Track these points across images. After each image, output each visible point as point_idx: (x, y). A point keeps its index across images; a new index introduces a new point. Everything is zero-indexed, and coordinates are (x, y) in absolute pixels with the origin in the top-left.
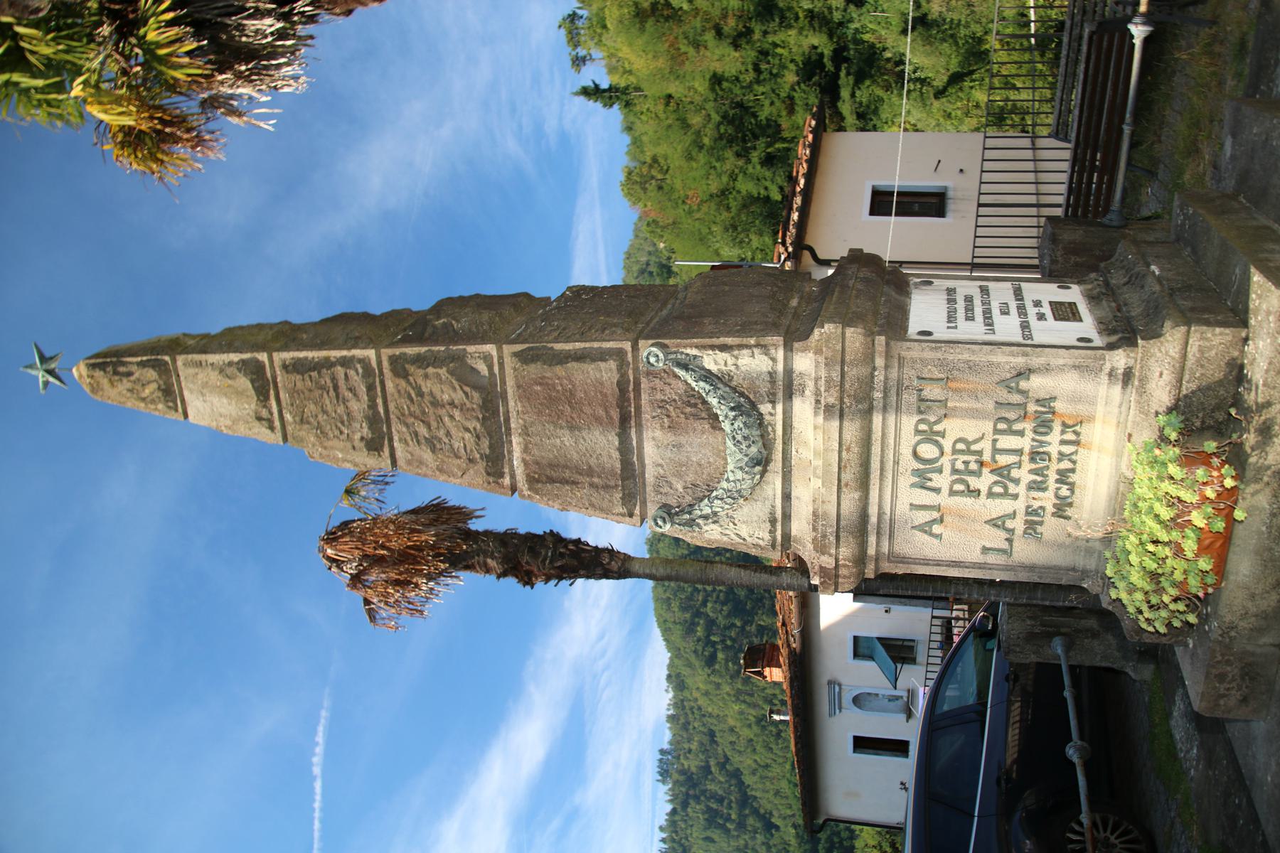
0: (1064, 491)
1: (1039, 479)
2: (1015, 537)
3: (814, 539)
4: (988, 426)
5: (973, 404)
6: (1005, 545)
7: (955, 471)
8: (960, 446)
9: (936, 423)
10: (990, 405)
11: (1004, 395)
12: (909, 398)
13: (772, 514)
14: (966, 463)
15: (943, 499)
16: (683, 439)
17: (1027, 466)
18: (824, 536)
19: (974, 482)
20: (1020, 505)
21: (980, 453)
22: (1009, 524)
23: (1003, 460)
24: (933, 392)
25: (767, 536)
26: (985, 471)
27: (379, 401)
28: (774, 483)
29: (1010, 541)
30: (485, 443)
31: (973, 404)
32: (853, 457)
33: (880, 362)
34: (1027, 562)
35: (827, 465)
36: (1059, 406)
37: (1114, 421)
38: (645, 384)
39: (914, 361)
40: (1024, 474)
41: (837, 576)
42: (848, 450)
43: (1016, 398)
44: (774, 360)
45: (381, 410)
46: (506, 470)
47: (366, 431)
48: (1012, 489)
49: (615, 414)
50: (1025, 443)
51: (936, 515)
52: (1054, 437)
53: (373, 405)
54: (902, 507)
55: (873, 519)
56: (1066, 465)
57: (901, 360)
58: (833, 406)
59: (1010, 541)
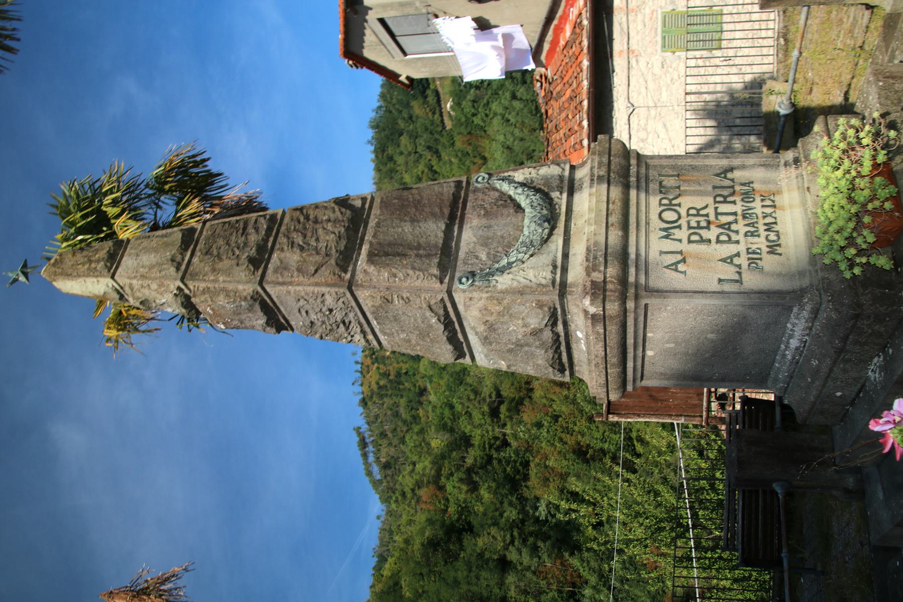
0: (772, 237)
1: (752, 229)
2: (742, 271)
4: (710, 200)
5: (698, 188)
6: (737, 277)
7: (690, 228)
8: (693, 212)
10: (710, 188)
11: (717, 181)
12: (653, 186)
14: (698, 222)
15: (684, 246)
16: (493, 222)
17: (741, 222)
18: (595, 258)
19: (705, 234)
20: (742, 248)
21: (707, 215)
22: (736, 261)
23: (724, 219)
24: (670, 182)
26: (712, 227)
27: (271, 239)
28: (558, 241)
29: (739, 273)
30: (343, 243)
31: (698, 188)
34: (755, 288)
36: (756, 186)
37: (796, 187)
38: (471, 197)
39: (655, 166)
41: (605, 290)
42: (613, 203)
45: (270, 244)
46: (350, 269)
47: (253, 252)
48: (734, 237)
49: (447, 211)
50: (738, 208)
51: (679, 257)
53: (265, 241)
54: (653, 254)
55: (633, 256)
56: (769, 220)
58: (603, 176)
59: (739, 273)
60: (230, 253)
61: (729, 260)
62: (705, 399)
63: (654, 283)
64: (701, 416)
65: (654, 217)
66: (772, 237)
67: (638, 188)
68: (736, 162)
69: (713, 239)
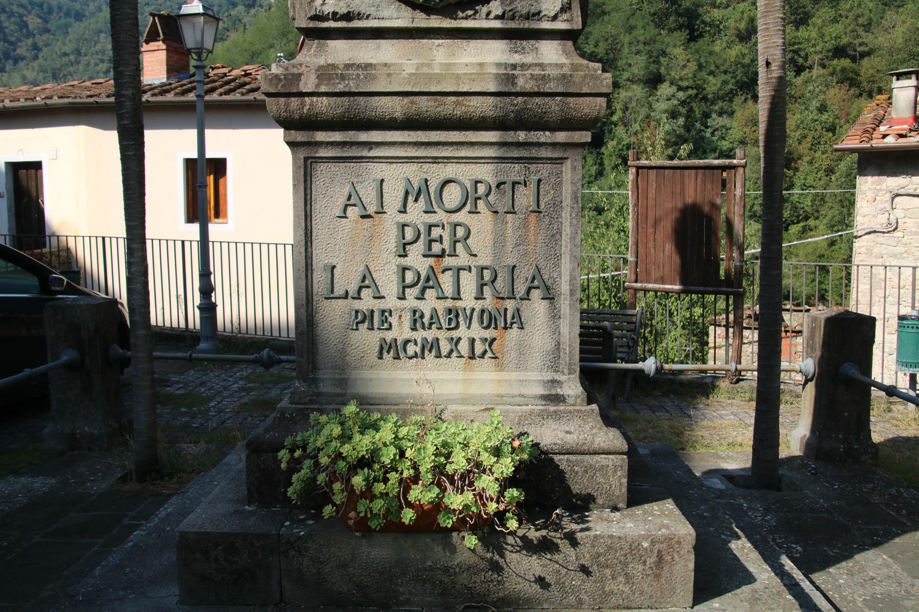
0: (411, 349)
1: (426, 320)
2: (350, 300)
3: (334, 66)
4: (485, 259)
6: (339, 291)
7: (430, 227)
8: (460, 232)
9: (489, 205)
10: (511, 262)
12: (515, 172)
13: (359, 16)
14: (441, 240)
15: (392, 217)
17: (441, 306)
18: (343, 78)
20: (391, 302)
21: (454, 254)
22: (365, 293)
23: (447, 281)
24: (525, 198)
25: (328, 9)
26: (431, 261)
29: (346, 296)
32: (449, 108)
33: (561, 137)
34: (318, 317)
35: (438, 78)
36: (514, 332)
37: (503, 392)
39: (559, 174)
40: (427, 306)
42: (458, 103)
43: (521, 289)
44: (555, 18)
48: (411, 293)
50: (468, 301)
52: (477, 331)
54: (379, 170)
55: (363, 137)
56: (445, 347)
57: (560, 160)
58: (514, 84)
59: (346, 296)
61: (367, 280)
63: (323, 172)
64: (636, 281)
65: (450, 170)
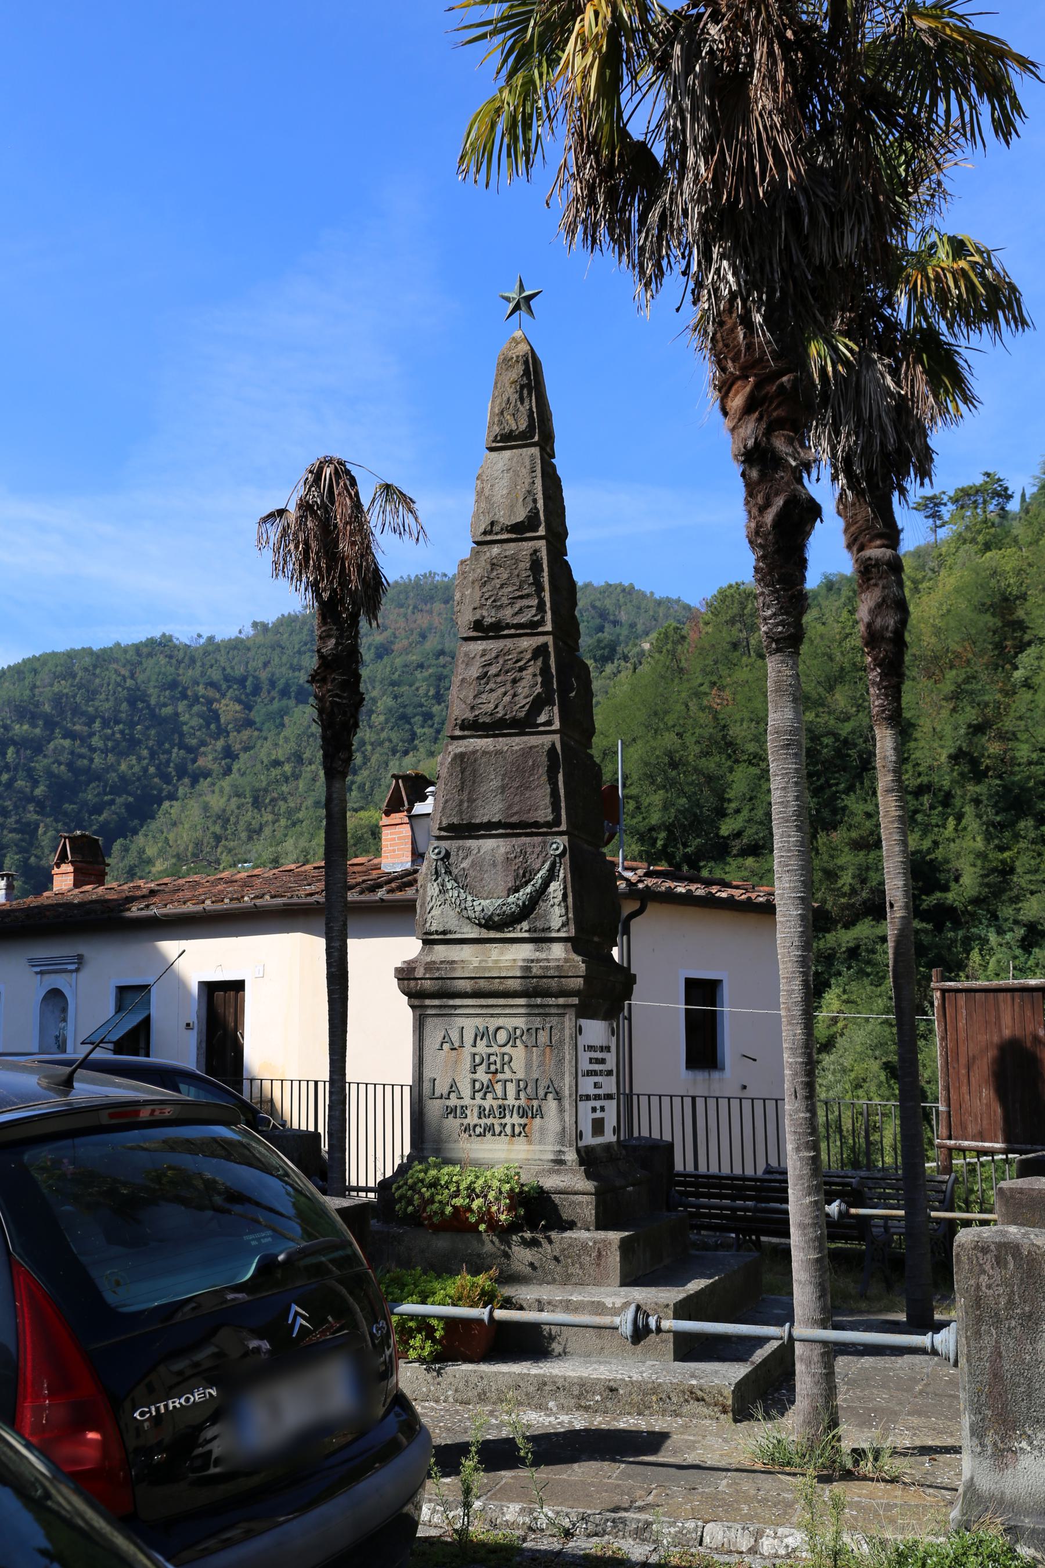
0: (478, 1130)
3: (434, 962)
4: (520, 1075)
5: (535, 1064)
6: (437, 1094)
7: (489, 1055)
8: (506, 1058)
9: (523, 1042)
10: (535, 1076)
11: (543, 1084)
12: (537, 1022)
13: (450, 932)
15: (468, 1049)
16: (499, 867)
17: (495, 1104)
18: (438, 969)
19: (482, 1069)
20: (467, 1101)
22: (452, 1095)
23: (499, 1087)
24: (543, 1037)
25: (433, 929)
27: (512, 631)
28: (473, 933)
29: (441, 1097)
30: (488, 720)
31: (535, 1064)
32: (496, 985)
33: (561, 1001)
35: (490, 969)
36: (538, 1120)
38: (537, 840)
39: (563, 1023)
40: (489, 1102)
41: (409, 979)
43: (541, 1093)
44: (559, 930)
45: (506, 632)
46: (466, 733)
47: (488, 620)
48: (478, 1095)
49: (514, 819)
50: (511, 1101)
51: (456, 1045)
52: (516, 1120)
53: (508, 626)
54: (461, 1022)
55: (451, 1002)
56: (497, 1129)
57: (563, 1015)
59: (441, 1097)
60: (487, 595)
61: (453, 1087)
62: (973, 1144)
63: (430, 1023)
64: (950, 1138)
65: (500, 1022)
66: (478, 1130)
67: (528, 1006)
68: (567, 1103)
69: (476, 1076)
